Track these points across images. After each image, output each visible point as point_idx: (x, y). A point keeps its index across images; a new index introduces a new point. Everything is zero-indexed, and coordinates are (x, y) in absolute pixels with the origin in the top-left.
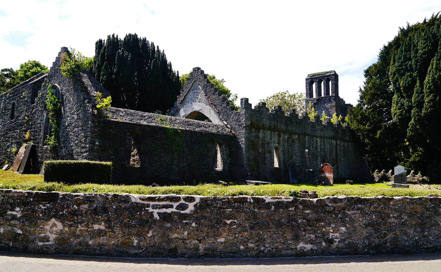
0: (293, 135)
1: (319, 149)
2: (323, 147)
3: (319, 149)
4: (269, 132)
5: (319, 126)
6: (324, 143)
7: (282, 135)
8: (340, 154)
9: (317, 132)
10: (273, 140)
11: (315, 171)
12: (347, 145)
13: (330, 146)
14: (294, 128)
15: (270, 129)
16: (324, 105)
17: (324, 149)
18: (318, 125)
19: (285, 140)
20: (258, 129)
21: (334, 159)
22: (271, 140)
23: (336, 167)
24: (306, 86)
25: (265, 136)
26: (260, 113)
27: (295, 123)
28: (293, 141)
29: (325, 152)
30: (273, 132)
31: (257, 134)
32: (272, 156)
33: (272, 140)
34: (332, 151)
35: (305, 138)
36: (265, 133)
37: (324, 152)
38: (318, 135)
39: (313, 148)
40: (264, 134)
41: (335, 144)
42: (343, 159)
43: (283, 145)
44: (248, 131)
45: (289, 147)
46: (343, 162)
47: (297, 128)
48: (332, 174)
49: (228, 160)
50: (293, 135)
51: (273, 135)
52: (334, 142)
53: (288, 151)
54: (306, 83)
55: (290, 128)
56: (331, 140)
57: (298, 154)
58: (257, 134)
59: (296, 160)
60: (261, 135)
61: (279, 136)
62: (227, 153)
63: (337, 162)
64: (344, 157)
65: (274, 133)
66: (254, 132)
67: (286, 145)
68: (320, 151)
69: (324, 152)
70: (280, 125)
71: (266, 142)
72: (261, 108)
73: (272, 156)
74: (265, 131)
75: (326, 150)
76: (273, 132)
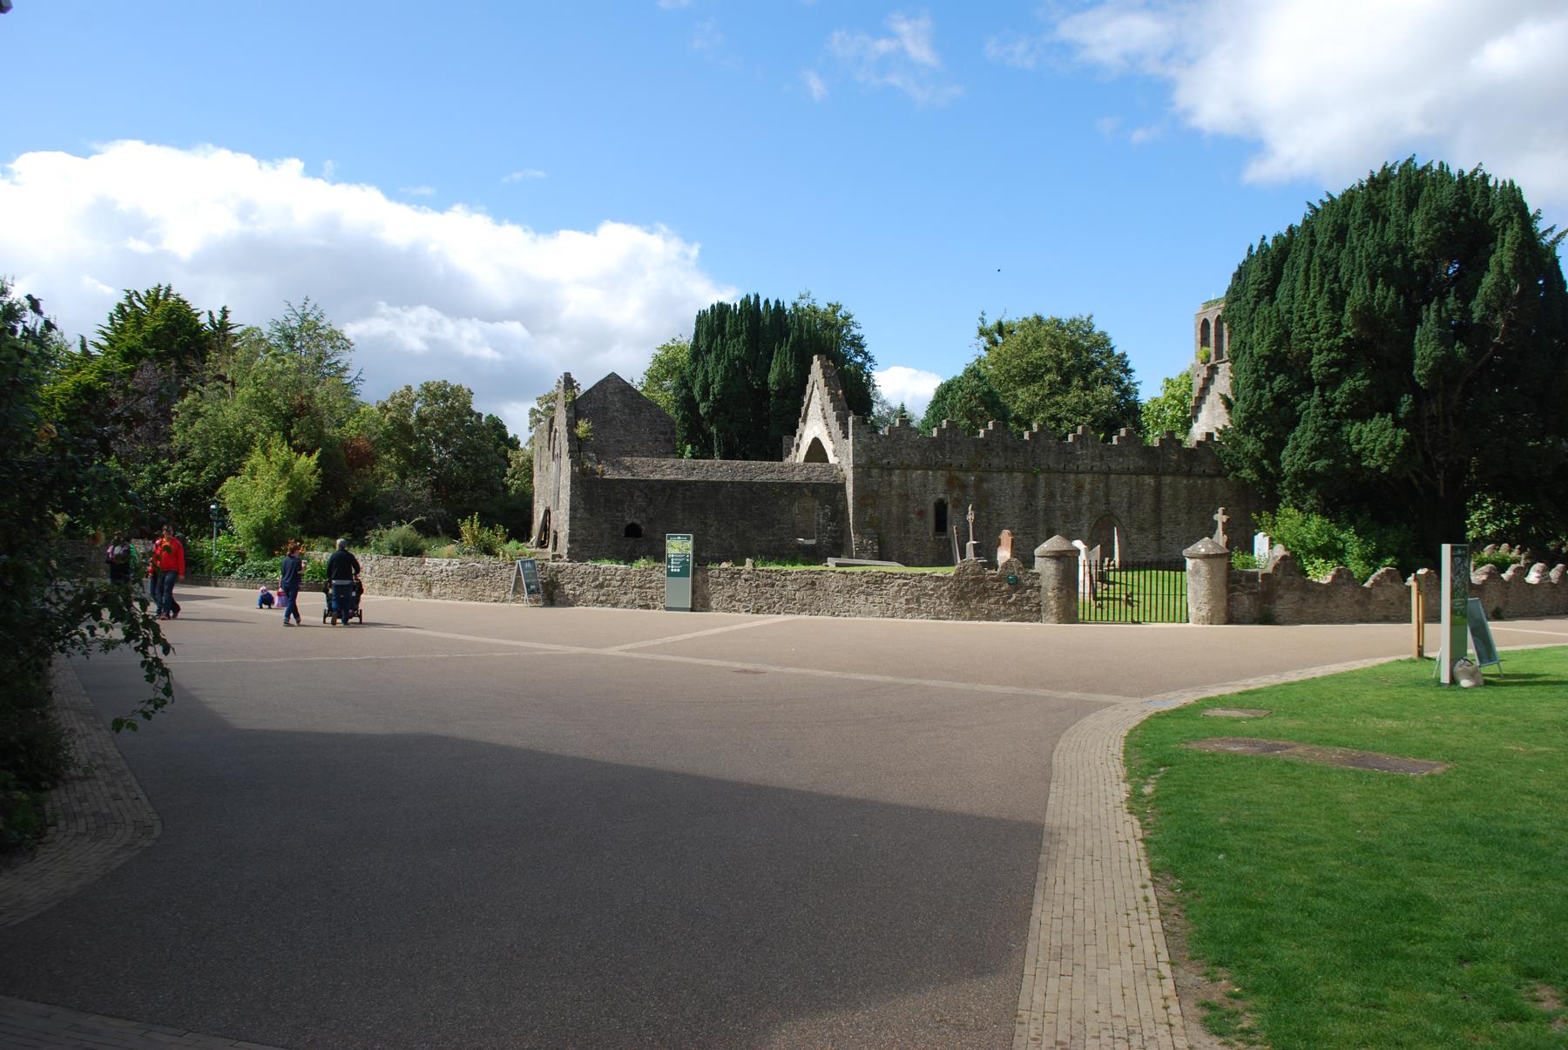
3: (1086, 499)
4: (919, 472)
5: (1087, 447)
6: (1107, 485)
9: (1080, 462)
12: (1203, 484)
13: (1130, 491)
15: (926, 466)
16: (1223, 382)
17: (1107, 495)
18: (1081, 448)
20: (889, 469)
22: (925, 486)
23: (1151, 536)
24: (1196, 335)
31: (886, 478)
37: (1108, 503)
38: (1081, 468)
39: (1062, 496)
40: (906, 477)
41: (1152, 484)
42: (1183, 517)
46: (1182, 525)
47: (1006, 459)
48: (1010, 550)
49: (829, 525)
50: (995, 474)
52: (1149, 480)
54: (1196, 326)
56: (1134, 477)
60: (895, 479)
62: (825, 514)
63: (1158, 523)
64: (1188, 513)
69: (1108, 503)
74: (908, 472)
76: (930, 473)
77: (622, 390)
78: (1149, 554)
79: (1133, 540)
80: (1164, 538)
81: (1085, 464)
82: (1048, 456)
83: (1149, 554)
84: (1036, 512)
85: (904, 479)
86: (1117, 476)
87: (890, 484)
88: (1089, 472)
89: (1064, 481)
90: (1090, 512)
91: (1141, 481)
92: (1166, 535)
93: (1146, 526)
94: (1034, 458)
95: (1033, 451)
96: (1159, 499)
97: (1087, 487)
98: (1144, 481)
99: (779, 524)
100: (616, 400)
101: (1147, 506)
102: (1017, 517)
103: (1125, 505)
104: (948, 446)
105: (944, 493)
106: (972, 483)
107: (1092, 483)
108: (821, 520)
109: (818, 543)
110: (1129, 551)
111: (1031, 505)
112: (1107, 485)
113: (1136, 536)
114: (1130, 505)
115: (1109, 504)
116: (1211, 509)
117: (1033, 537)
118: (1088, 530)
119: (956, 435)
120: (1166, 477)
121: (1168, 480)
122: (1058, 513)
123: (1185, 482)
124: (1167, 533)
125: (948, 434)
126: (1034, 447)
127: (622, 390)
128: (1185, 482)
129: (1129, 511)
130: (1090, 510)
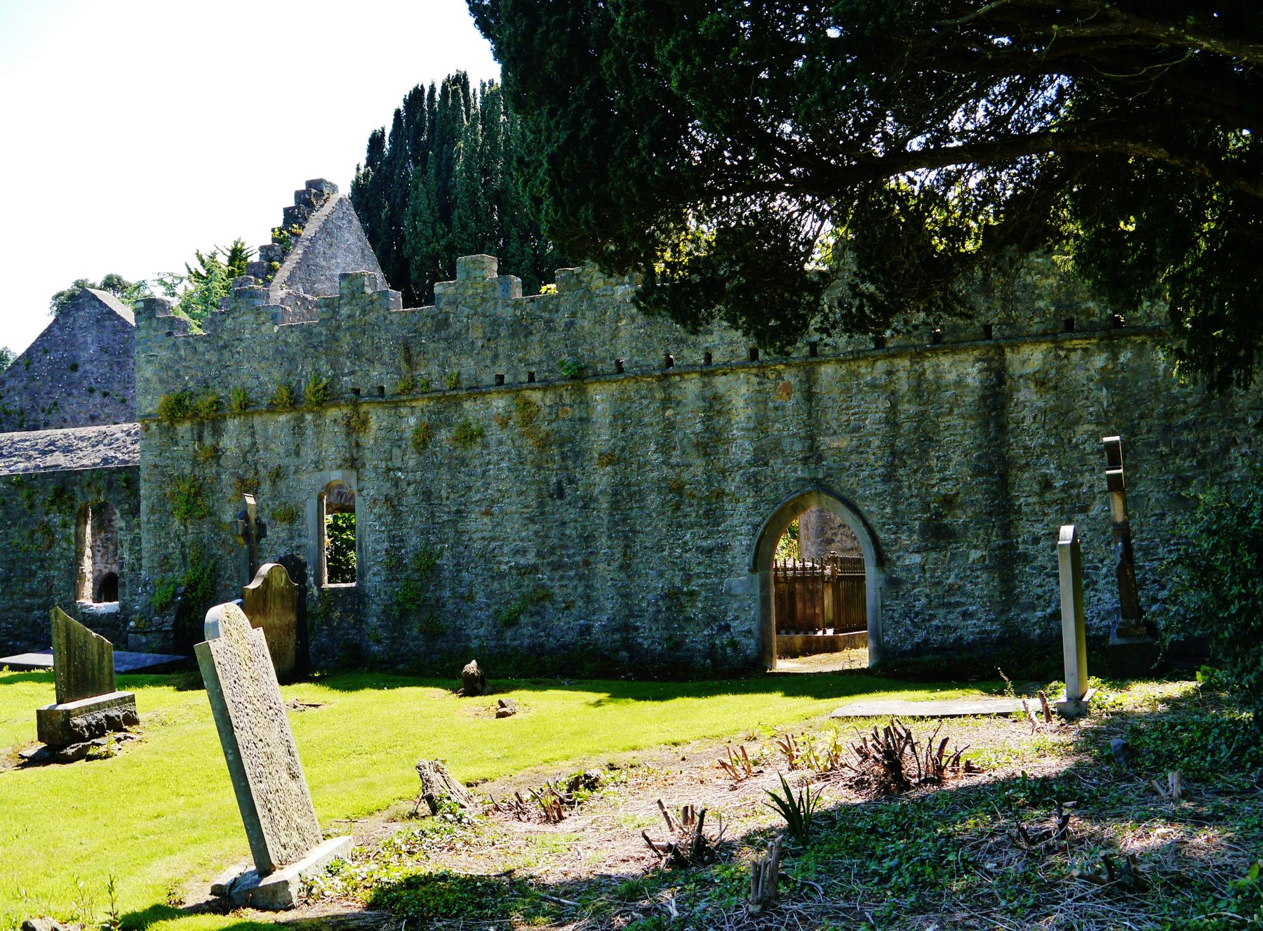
0: (467, 405)
1: (741, 449)
2: (788, 428)
3: (741, 449)
4: (282, 418)
7: (377, 418)
8: (1064, 445)
10: (309, 454)
11: (692, 594)
14: (467, 366)
15: (293, 401)
19: (398, 442)
20: (214, 418)
21: (948, 502)
22: (297, 454)
23: (975, 555)
25: (254, 444)
26: (221, 343)
27: (476, 334)
28: (469, 436)
29: (820, 458)
30: (309, 417)
32: (300, 536)
33: (303, 453)
34: (926, 439)
35: (586, 404)
36: (258, 428)
37: (813, 455)
38: (717, 357)
39: (665, 448)
40: (253, 434)
43: (389, 470)
44: (155, 441)
45: (429, 475)
47: (496, 356)
50: (467, 405)
51: (309, 432)
53: (427, 495)
55: (435, 370)
56: (903, 363)
57: (512, 505)
58: (208, 441)
59: (493, 539)
61: (355, 426)
65: (319, 416)
66: (188, 436)
67: (412, 463)
68: (760, 458)
69: (813, 455)
70: (353, 373)
71: (263, 473)
72: (224, 321)
73: (300, 536)
74: (257, 420)
75: (832, 443)
76: (309, 417)
77: (98, 320)
78: (966, 615)
79: (908, 569)
80: (1025, 558)
81: (731, 343)
82: (615, 335)
83: (966, 615)
84: (587, 503)
85: (247, 441)
86: (843, 370)
87: (216, 453)
88: (742, 365)
89: (666, 402)
90: (758, 491)
91: (929, 375)
92: (1031, 550)
93: (959, 518)
94: (575, 345)
95: (570, 325)
96: (1002, 428)
97: (741, 412)
98: (939, 376)
99: (42, 567)
100: (89, 340)
101: (956, 458)
102: (532, 520)
103: (875, 457)
104: (346, 342)
105: (340, 466)
106: (409, 434)
107: (759, 399)
108: (126, 556)
109: (123, 607)
110: (899, 606)
111: (571, 481)
112: (810, 396)
113: (917, 558)
114: (895, 457)
115: (820, 458)
116: (1214, 445)
117: (581, 577)
118: (748, 548)
119: (364, 312)
120: (1026, 350)
121: (1030, 358)
122: (653, 500)
123: (1099, 360)
124: (1036, 540)
125: (345, 311)
126: (574, 314)
127: (98, 320)
128: (1099, 360)
129: (887, 479)
130: (754, 482)
